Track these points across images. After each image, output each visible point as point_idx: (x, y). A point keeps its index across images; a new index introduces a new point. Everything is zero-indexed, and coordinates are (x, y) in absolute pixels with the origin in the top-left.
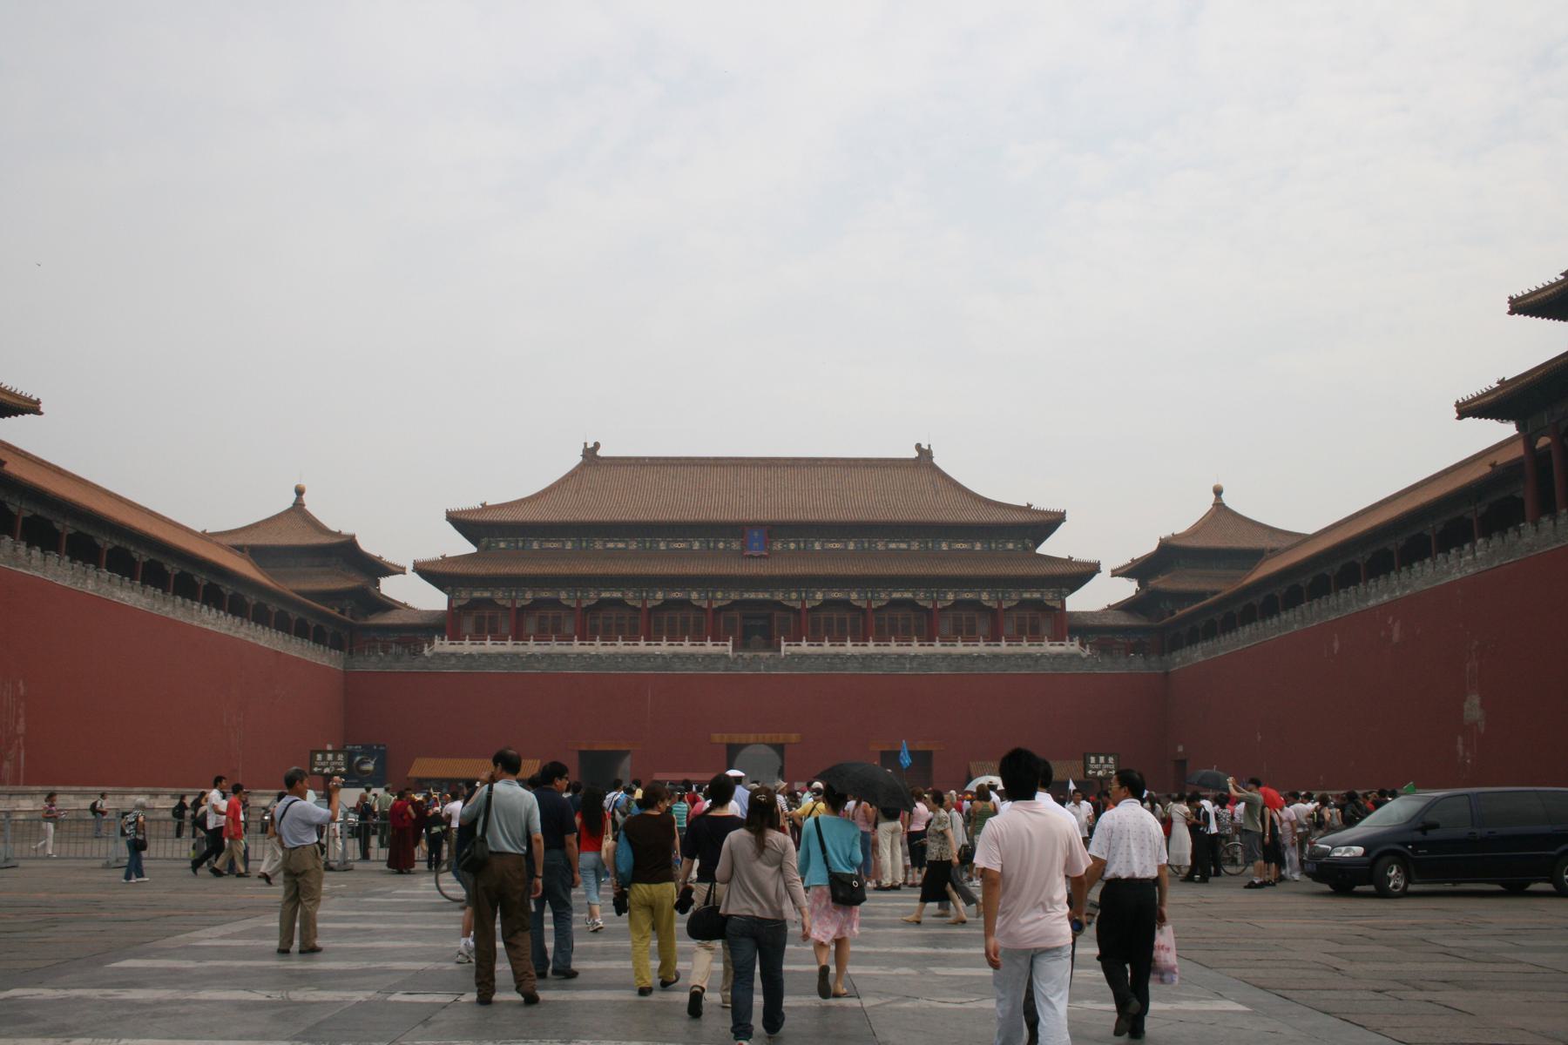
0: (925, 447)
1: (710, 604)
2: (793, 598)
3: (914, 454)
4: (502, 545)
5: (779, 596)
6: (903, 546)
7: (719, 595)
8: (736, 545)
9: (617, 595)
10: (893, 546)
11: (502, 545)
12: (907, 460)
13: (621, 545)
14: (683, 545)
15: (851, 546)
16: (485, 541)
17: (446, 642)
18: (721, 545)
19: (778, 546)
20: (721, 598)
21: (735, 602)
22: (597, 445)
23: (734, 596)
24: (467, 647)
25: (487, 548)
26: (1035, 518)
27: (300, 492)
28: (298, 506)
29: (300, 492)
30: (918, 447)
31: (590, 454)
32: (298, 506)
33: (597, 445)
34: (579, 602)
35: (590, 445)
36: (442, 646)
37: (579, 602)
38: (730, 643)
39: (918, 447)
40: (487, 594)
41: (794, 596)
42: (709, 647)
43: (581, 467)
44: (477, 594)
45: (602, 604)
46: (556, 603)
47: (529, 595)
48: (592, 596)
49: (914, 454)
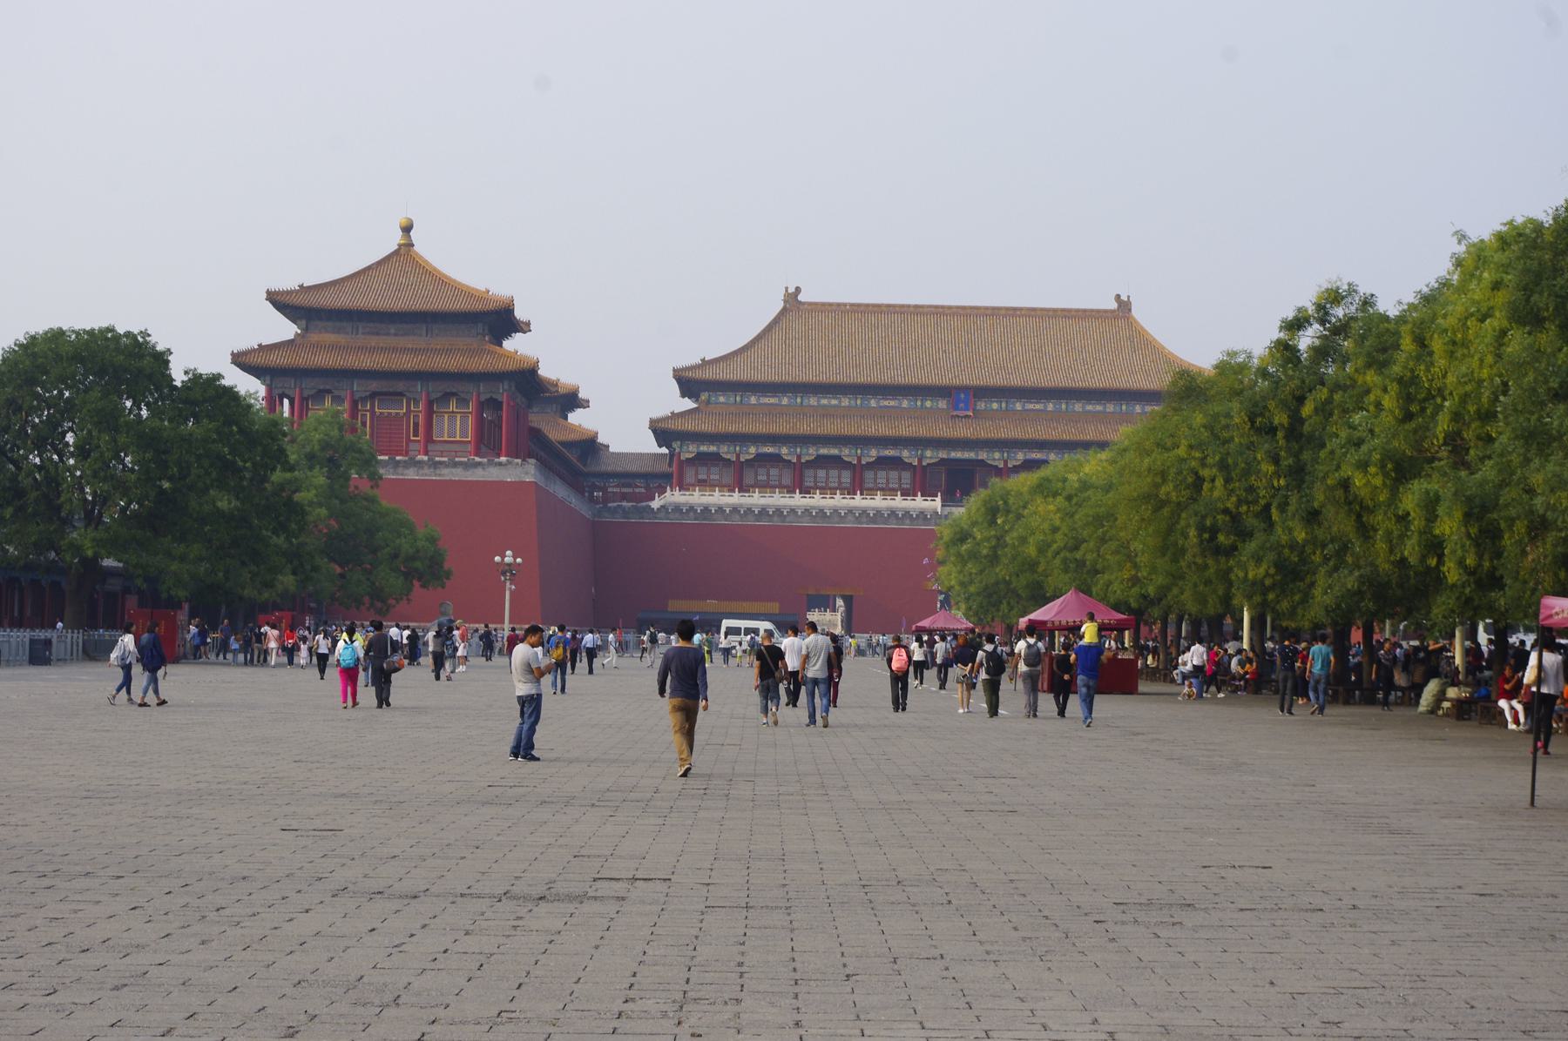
0: (1124, 298)
1: (920, 461)
2: (996, 458)
3: (1114, 306)
4: (722, 399)
5: (983, 455)
6: (1099, 408)
7: (928, 453)
8: (942, 404)
9: (834, 451)
10: (1089, 407)
12: (1106, 311)
13: (834, 402)
14: (892, 403)
15: (1050, 407)
16: (704, 396)
17: (677, 493)
18: (928, 404)
19: (981, 405)
20: (931, 456)
22: (798, 290)
23: (943, 455)
24: (697, 498)
25: (708, 402)
30: (1118, 297)
31: (792, 299)
33: (798, 290)
34: (799, 457)
35: (791, 290)
36: (674, 496)
37: (799, 457)
38: (938, 499)
40: (713, 449)
41: (997, 455)
42: (919, 503)
43: (784, 311)
44: (704, 448)
45: (819, 457)
46: (776, 459)
47: (753, 450)
48: (811, 453)
49: (1114, 306)
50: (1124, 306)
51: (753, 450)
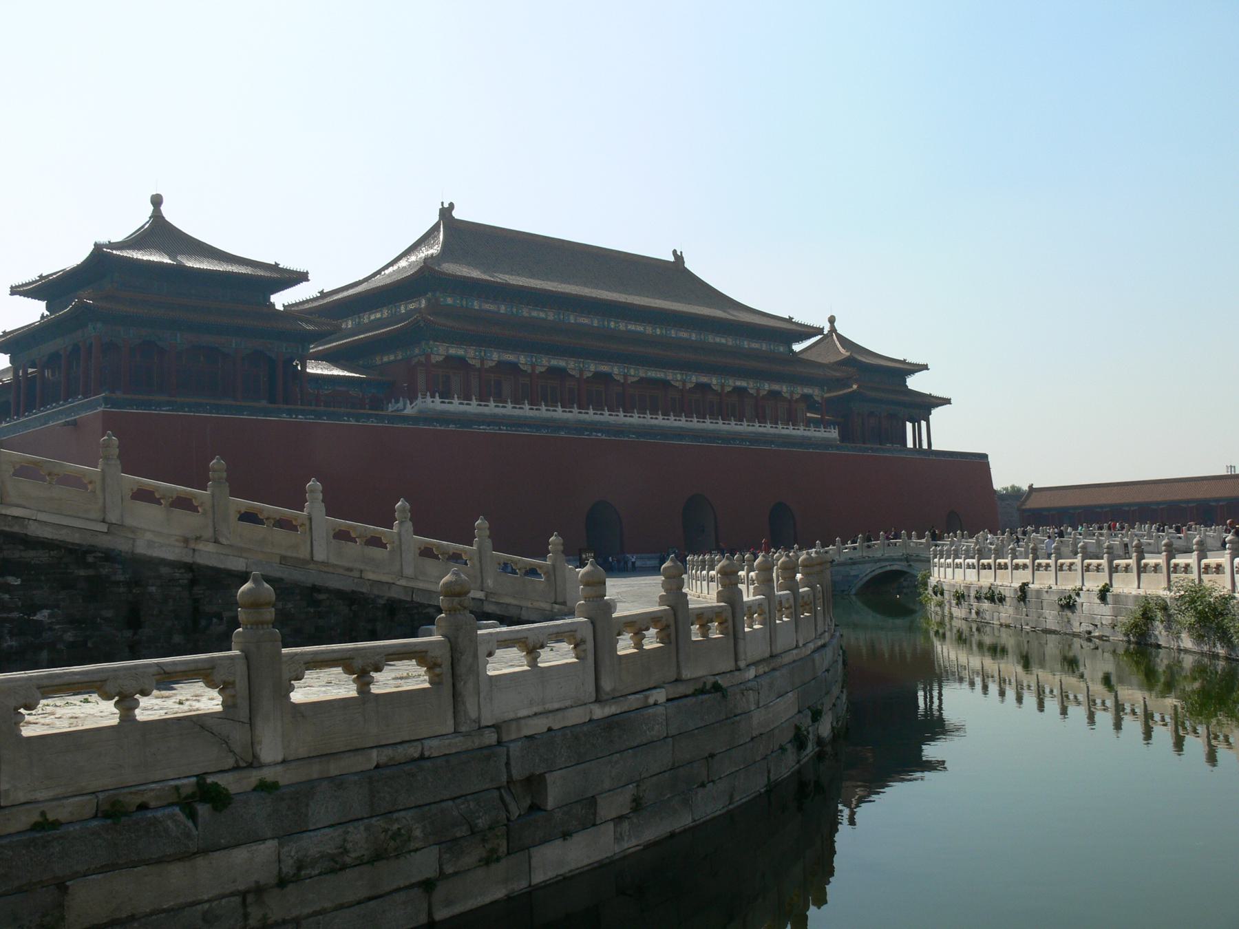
3: (672, 259)
4: (449, 301)
5: (670, 377)
7: (632, 372)
11: (449, 301)
17: (438, 400)
20: (636, 373)
21: (642, 380)
22: (452, 205)
23: (642, 374)
26: (793, 327)
27: (157, 201)
28: (157, 217)
29: (157, 201)
30: (675, 252)
31: (446, 213)
32: (157, 218)
33: (452, 205)
35: (446, 205)
39: (675, 252)
40: (461, 352)
41: (679, 377)
47: (495, 356)
49: (672, 259)
50: (679, 258)
51: (495, 356)
